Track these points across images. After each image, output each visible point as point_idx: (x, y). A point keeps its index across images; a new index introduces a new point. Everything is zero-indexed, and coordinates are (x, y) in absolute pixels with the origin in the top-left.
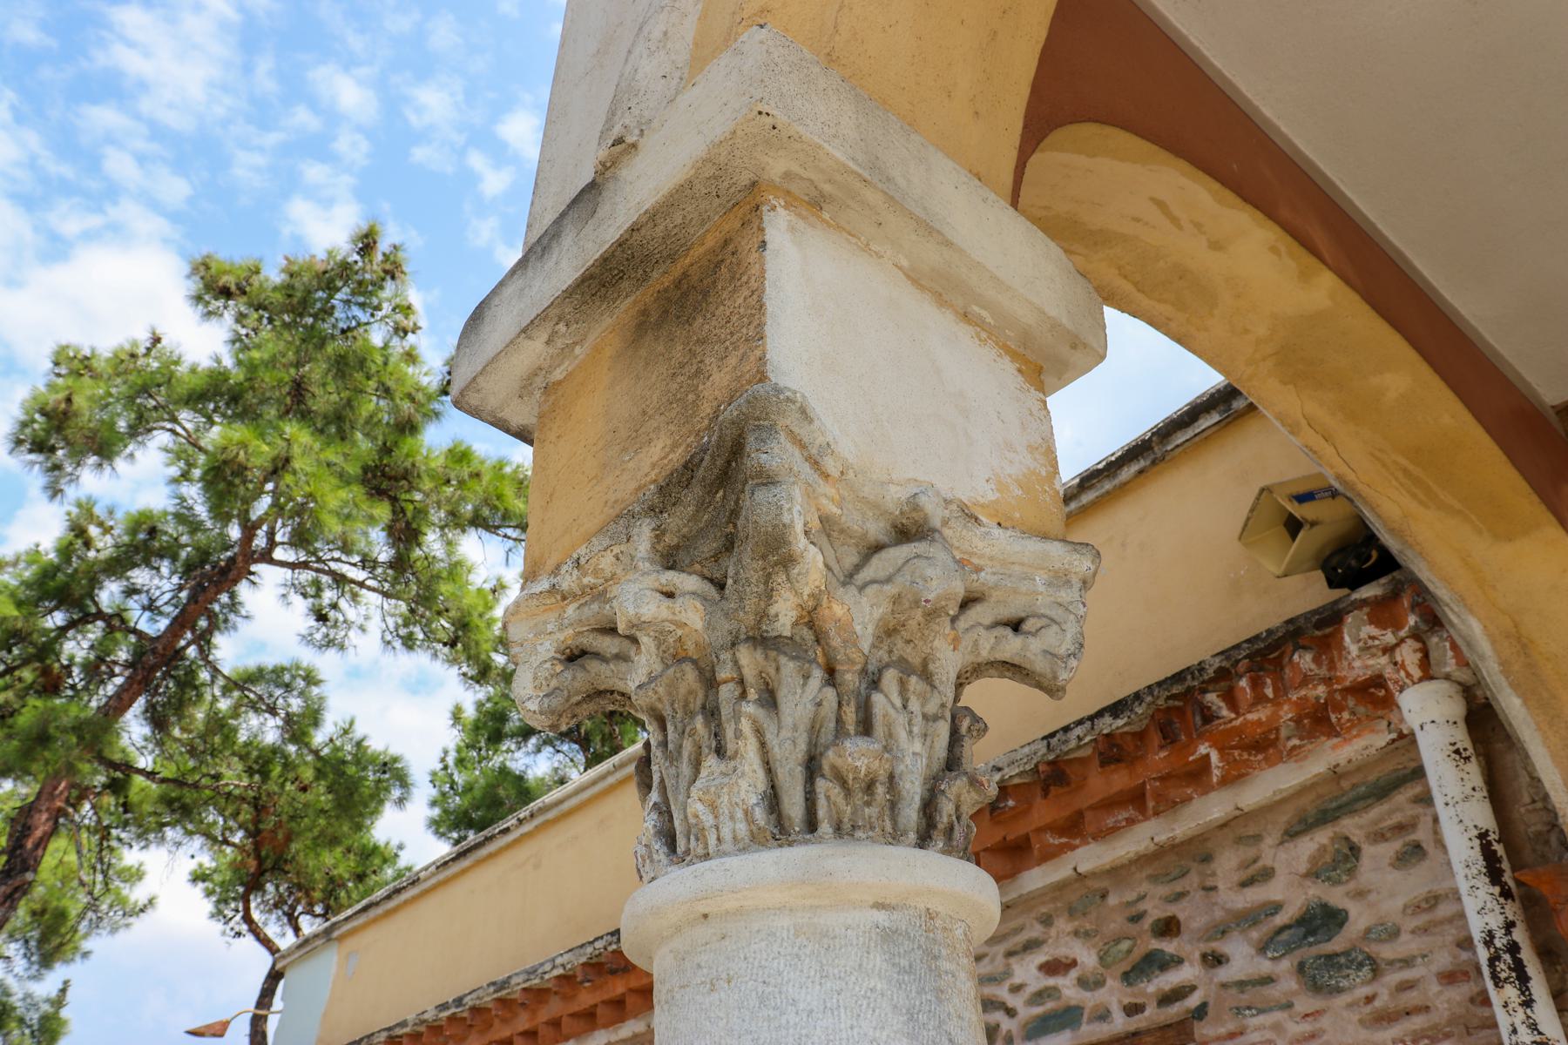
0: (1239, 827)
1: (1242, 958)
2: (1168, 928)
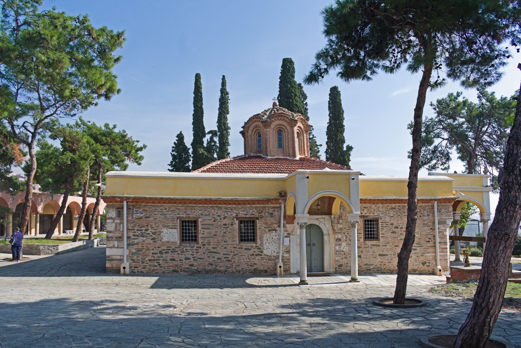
0: (269, 207)
1: (267, 214)
2: (262, 211)
